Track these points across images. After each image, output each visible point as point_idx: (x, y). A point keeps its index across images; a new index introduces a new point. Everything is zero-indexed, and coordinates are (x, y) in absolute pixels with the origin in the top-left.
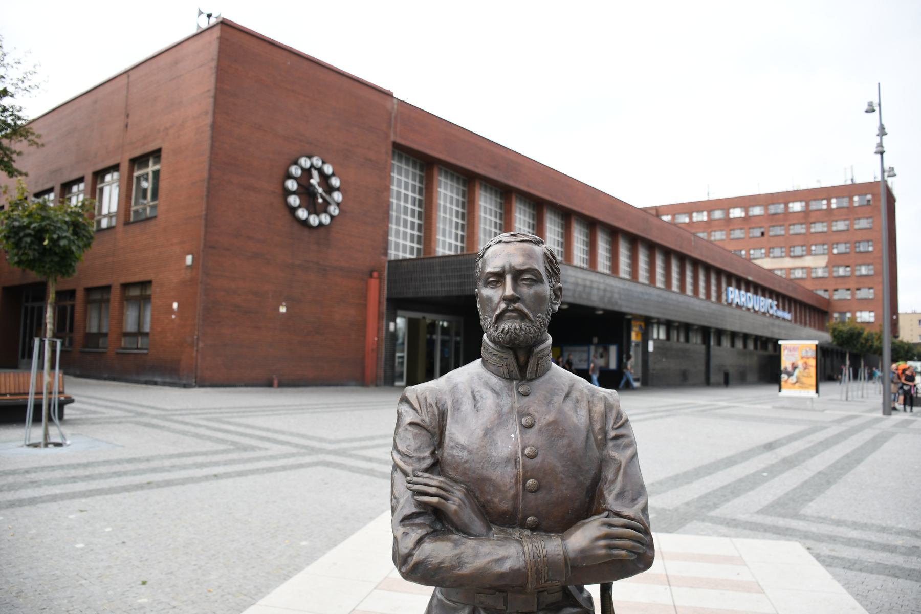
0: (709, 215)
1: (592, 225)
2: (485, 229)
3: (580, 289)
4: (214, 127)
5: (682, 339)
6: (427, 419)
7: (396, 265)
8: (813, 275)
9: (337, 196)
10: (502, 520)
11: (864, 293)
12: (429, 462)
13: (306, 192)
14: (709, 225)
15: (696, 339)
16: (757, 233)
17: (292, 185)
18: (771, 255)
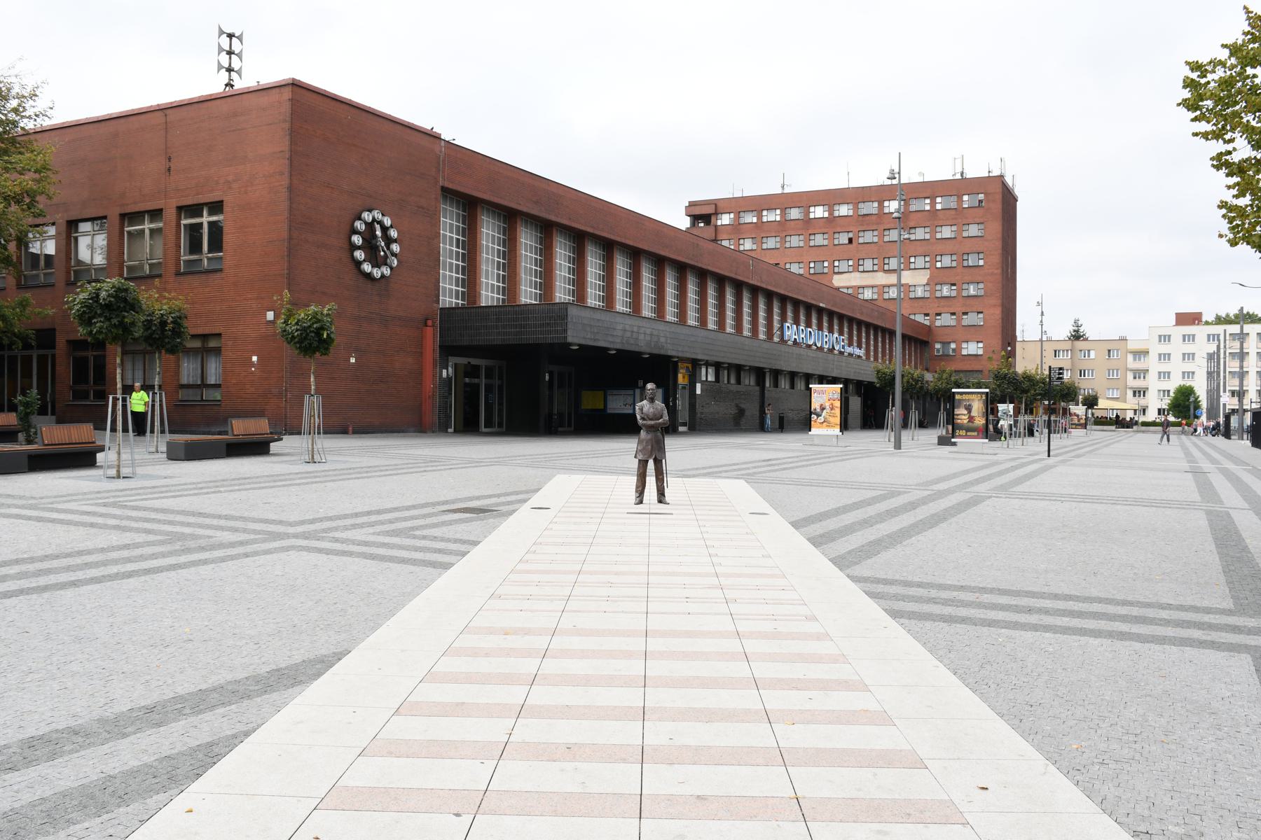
0: (783, 214)
1: (635, 255)
3: (628, 334)
4: (291, 188)
5: (733, 381)
7: (447, 313)
8: (912, 295)
9: (395, 248)
11: (972, 319)
13: (370, 246)
14: (782, 228)
15: (749, 381)
16: (844, 239)
17: (357, 240)
18: (861, 268)
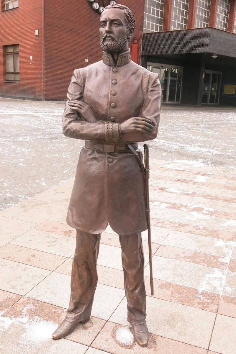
2: (199, 15)
6: (79, 81)
7: (148, 36)
10: (100, 117)
12: (78, 97)
